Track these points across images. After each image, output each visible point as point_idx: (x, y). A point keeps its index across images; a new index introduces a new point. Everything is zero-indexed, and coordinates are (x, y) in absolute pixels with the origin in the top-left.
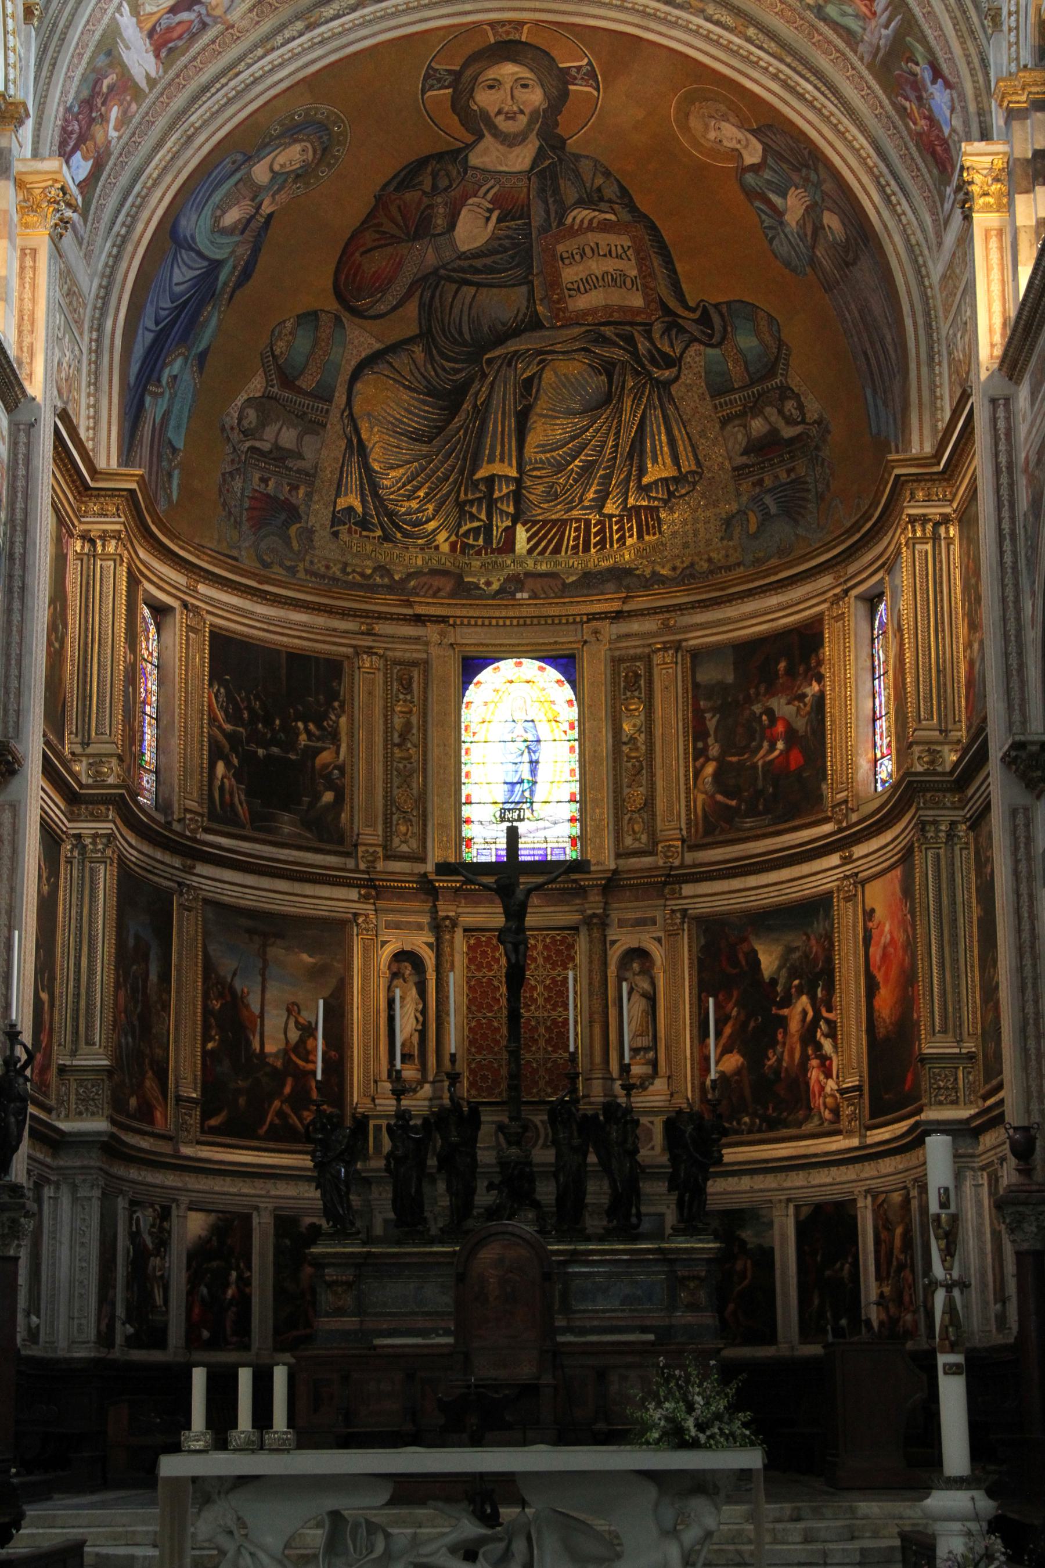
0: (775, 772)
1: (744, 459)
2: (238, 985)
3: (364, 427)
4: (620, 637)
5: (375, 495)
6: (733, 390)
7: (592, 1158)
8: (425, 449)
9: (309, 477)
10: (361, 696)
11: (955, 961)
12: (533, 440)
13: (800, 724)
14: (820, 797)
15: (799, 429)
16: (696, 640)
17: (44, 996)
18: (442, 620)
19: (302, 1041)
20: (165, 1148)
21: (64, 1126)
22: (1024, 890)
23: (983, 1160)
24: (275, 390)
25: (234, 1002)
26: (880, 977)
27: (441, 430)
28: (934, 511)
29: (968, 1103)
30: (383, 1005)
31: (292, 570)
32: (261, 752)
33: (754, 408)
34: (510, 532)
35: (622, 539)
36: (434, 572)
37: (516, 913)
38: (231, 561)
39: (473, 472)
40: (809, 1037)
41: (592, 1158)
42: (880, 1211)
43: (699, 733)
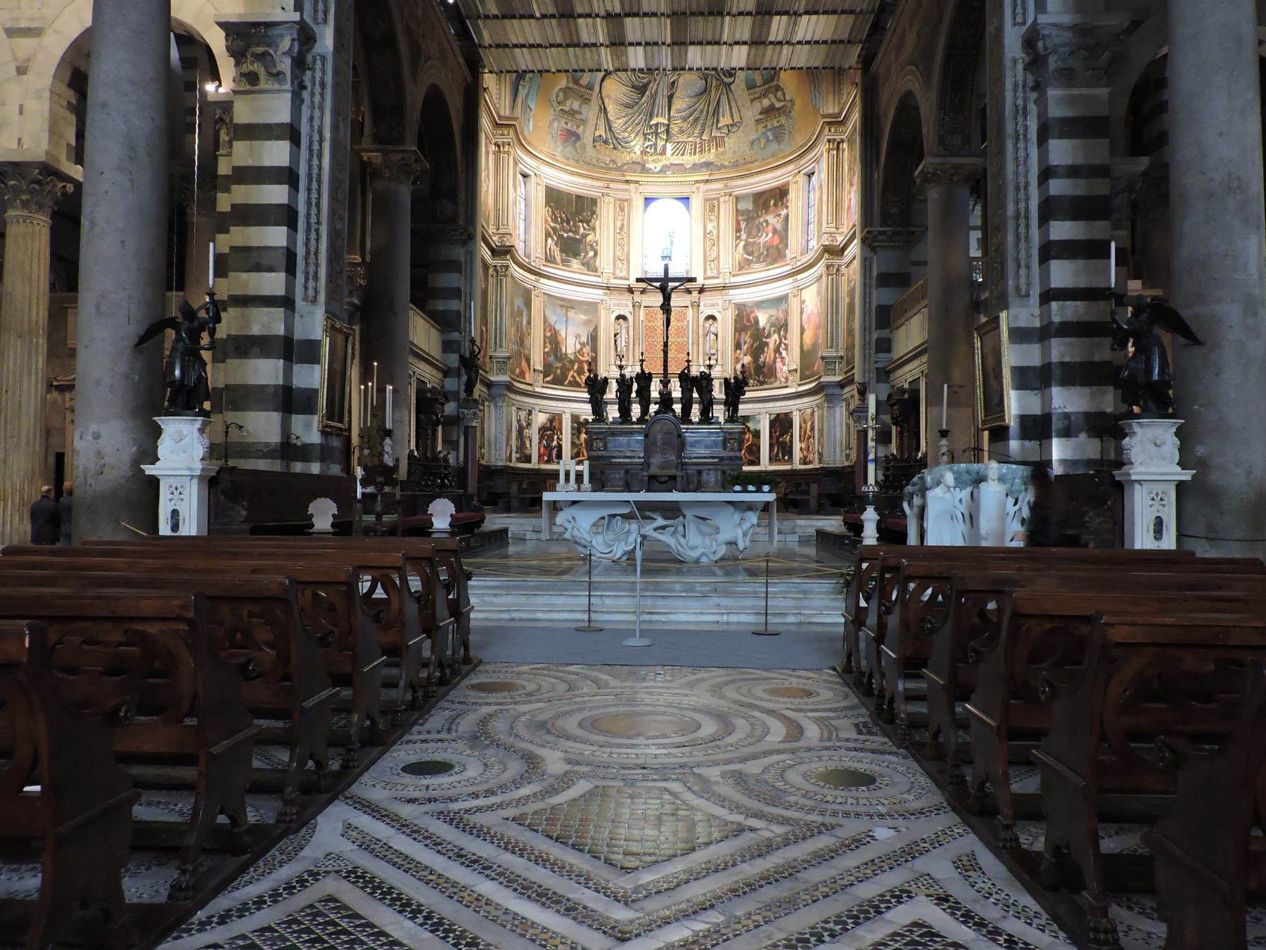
0: (768, 247)
1: (760, 117)
2: (557, 327)
3: (606, 101)
4: (707, 191)
5: (610, 130)
6: (756, 87)
8: (630, 111)
9: (584, 122)
11: (837, 320)
13: (779, 227)
14: (785, 256)
15: (782, 104)
16: (738, 192)
17: (484, 328)
18: (637, 182)
19: (581, 349)
21: (492, 379)
22: (867, 291)
23: (844, 397)
24: (571, 85)
26: (806, 326)
27: (637, 103)
28: (838, 138)
29: (839, 375)
32: (565, 235)
33: (764, 95)
35: (709, 149)
36: (634, 163)
37: (667, 299)
38: (553, 156)
39: (651, 119)
40: (777, 350)
41: (695, 395)
43: (738, 230)
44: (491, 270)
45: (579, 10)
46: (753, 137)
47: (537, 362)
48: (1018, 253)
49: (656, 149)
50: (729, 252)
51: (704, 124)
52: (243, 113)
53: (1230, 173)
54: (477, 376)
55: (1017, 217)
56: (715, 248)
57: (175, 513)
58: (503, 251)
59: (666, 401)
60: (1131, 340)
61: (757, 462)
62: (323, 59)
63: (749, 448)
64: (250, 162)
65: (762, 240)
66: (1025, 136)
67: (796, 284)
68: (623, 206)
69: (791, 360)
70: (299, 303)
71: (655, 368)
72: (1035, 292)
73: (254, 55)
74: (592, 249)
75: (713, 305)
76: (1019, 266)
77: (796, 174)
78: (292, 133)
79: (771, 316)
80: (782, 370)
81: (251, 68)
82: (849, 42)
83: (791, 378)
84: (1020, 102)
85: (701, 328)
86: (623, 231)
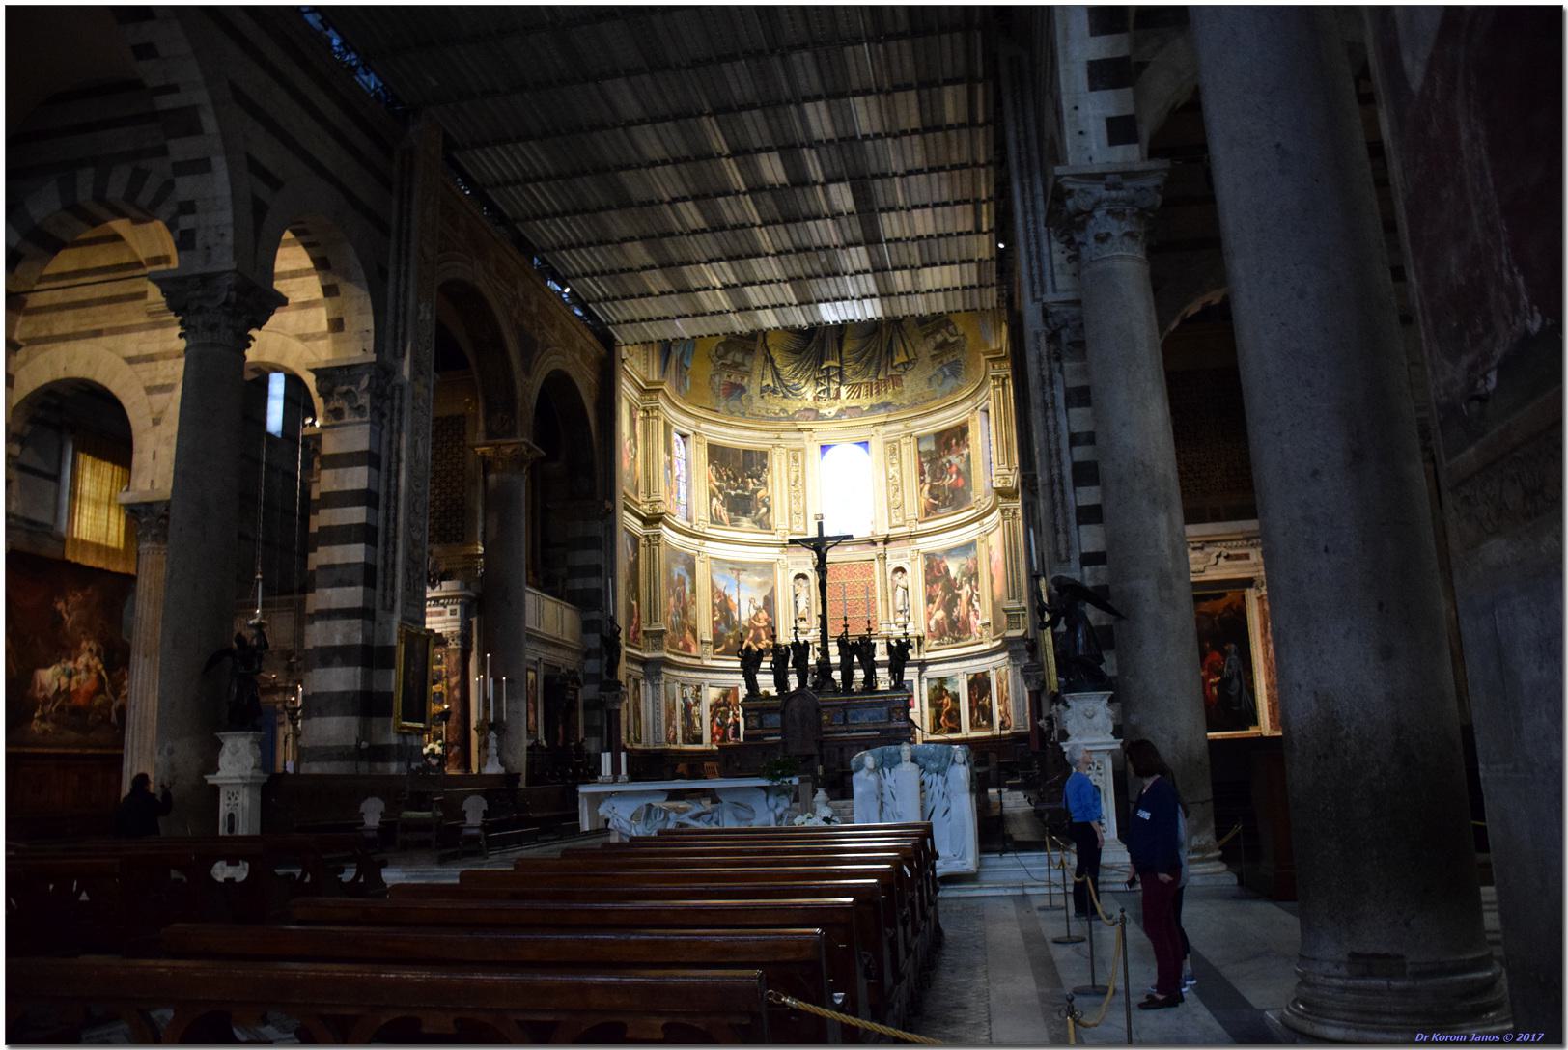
0: (953, 489)
2: (727, 592)
3: (772, 350)
5: (779, 378)
7: (856, 659)
8: (798, 357)
10: (776, 466)
11: (1017, 568)
12: (845, 350)
13: (962, 467)
17: (635, 603)
18: (811, 430)
20: (697, 662)
21: (646, 656)
25: (725, 599)
30: (792, 597)
31: (744, 414)
33: (937, 331)
34: (838, 390)
36: (806, 410)
39: (822, 363)
40: (970, 602)
41: (856, 659)
42: (998, 674)
43: (922, 473)
44: (642, 541)
45: (695, 284)
46: (932, 373)
47: (705, 631)
48: (1055, 520)
49: (829, 394)
50: (914, 498)
51: (879, 363)
52: (330, 445)
53: (1134, 458)
54: (619, 656)
55: (1051, 483)
56: (899, 493)
57: (231, 816)
58: (653, 520)
59: (825, 667)
60: (1063, 618)
61: (957, 730)
62: (401, 389)
63: (949, 713)
64: (335, 488)
65: (947, 482)
66: (1053, 403)
67: (982, 529)
68: (796, 455)
69: (981, 616)
70: (379, 612)
71: (813, 635)
72: (1075, 557)
73: (339, 394)
74: (765, 505)
75: (900, 556)
76: (1057, 532)
77: (973, 412)
78: (370, 459)
79: (962, 565)
80: (976, 623)
81: (337, 405)
82: (981, 286)
83: (985, 633)
84: (1046, 373)
85: (889, 582)
86: (798, 484)
